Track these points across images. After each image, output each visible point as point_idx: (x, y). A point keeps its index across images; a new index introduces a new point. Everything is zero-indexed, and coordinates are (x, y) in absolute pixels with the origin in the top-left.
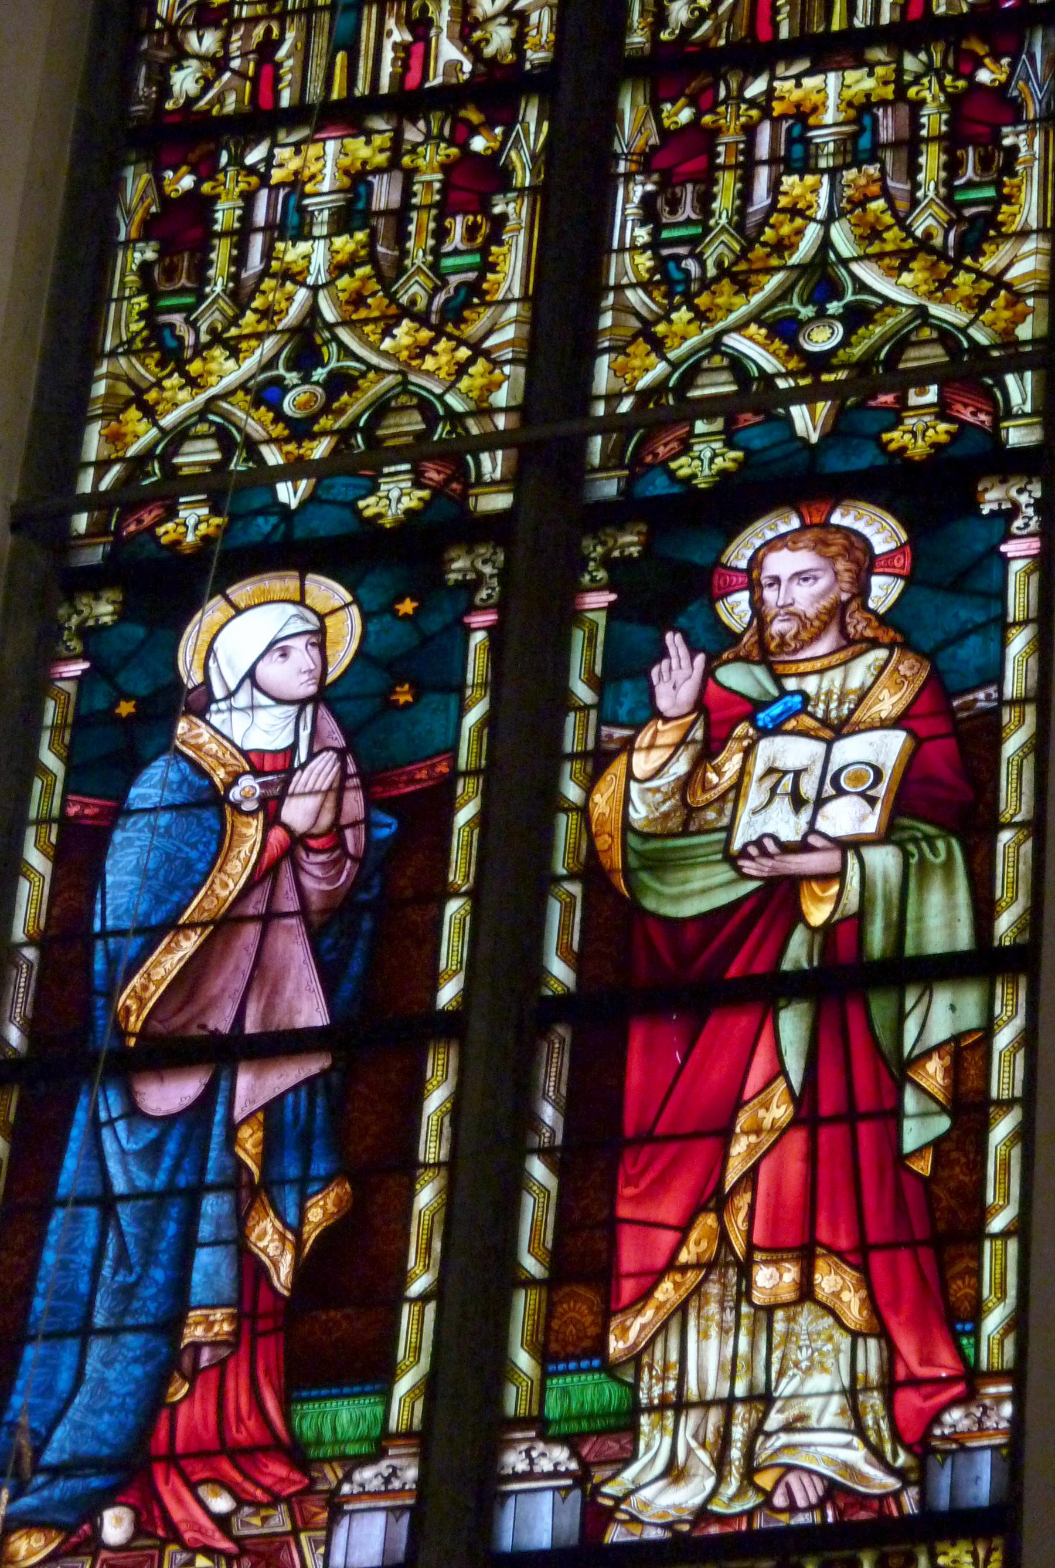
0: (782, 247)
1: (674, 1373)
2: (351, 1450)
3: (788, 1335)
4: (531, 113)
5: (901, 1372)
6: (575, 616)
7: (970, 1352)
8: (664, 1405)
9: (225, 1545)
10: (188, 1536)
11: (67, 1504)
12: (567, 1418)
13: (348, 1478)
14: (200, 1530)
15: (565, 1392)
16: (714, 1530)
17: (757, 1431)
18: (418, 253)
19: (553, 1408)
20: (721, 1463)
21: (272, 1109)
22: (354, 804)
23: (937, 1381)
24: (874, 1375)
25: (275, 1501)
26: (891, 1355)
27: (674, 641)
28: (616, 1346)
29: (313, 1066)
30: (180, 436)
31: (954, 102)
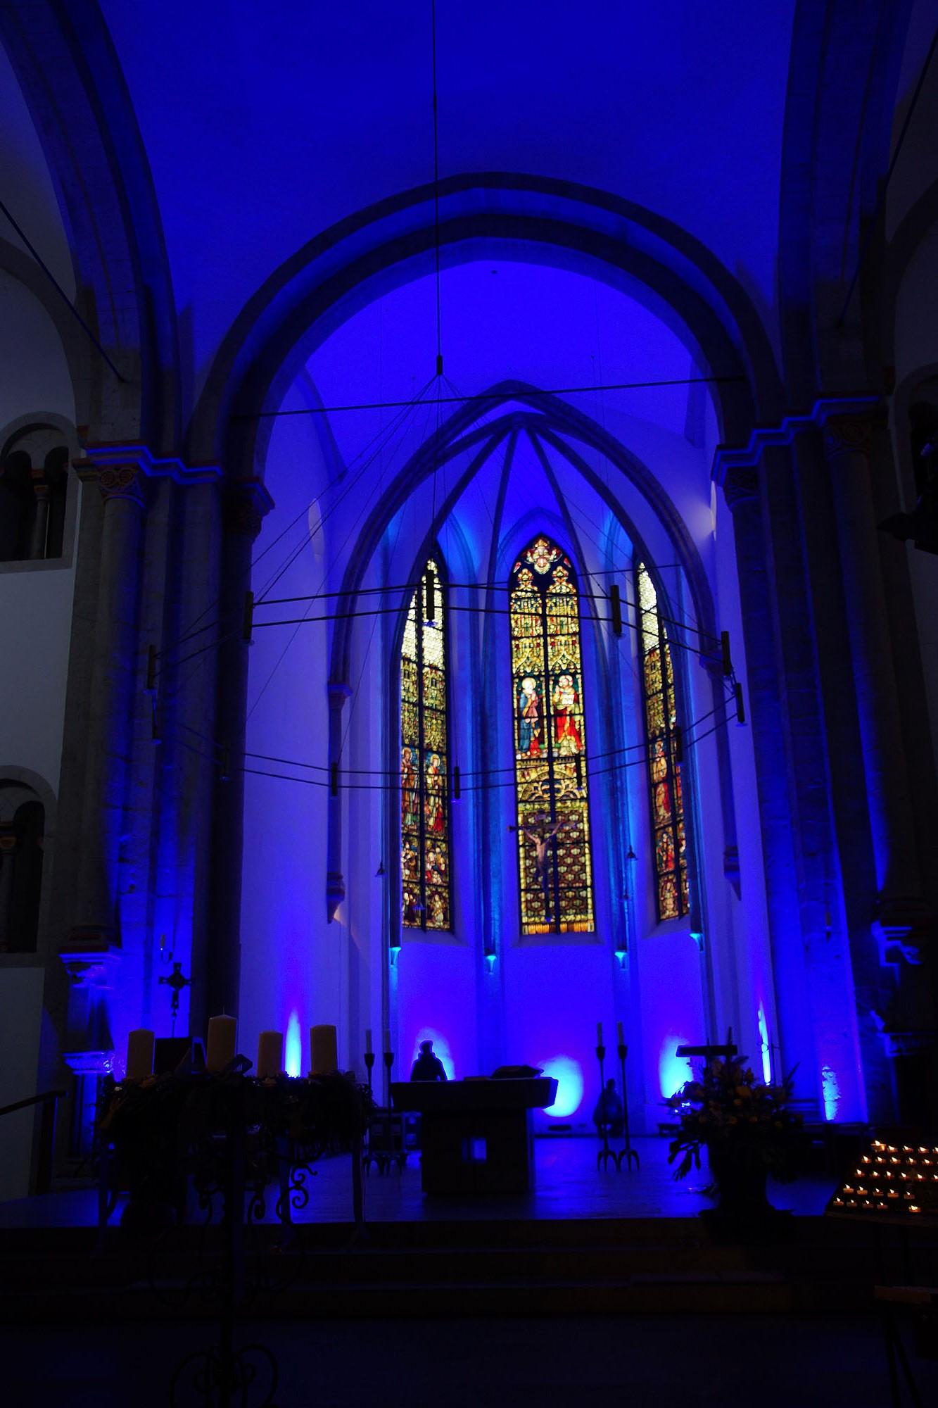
4: (542, 639)
18: (535, 651)
29: (537, 719)
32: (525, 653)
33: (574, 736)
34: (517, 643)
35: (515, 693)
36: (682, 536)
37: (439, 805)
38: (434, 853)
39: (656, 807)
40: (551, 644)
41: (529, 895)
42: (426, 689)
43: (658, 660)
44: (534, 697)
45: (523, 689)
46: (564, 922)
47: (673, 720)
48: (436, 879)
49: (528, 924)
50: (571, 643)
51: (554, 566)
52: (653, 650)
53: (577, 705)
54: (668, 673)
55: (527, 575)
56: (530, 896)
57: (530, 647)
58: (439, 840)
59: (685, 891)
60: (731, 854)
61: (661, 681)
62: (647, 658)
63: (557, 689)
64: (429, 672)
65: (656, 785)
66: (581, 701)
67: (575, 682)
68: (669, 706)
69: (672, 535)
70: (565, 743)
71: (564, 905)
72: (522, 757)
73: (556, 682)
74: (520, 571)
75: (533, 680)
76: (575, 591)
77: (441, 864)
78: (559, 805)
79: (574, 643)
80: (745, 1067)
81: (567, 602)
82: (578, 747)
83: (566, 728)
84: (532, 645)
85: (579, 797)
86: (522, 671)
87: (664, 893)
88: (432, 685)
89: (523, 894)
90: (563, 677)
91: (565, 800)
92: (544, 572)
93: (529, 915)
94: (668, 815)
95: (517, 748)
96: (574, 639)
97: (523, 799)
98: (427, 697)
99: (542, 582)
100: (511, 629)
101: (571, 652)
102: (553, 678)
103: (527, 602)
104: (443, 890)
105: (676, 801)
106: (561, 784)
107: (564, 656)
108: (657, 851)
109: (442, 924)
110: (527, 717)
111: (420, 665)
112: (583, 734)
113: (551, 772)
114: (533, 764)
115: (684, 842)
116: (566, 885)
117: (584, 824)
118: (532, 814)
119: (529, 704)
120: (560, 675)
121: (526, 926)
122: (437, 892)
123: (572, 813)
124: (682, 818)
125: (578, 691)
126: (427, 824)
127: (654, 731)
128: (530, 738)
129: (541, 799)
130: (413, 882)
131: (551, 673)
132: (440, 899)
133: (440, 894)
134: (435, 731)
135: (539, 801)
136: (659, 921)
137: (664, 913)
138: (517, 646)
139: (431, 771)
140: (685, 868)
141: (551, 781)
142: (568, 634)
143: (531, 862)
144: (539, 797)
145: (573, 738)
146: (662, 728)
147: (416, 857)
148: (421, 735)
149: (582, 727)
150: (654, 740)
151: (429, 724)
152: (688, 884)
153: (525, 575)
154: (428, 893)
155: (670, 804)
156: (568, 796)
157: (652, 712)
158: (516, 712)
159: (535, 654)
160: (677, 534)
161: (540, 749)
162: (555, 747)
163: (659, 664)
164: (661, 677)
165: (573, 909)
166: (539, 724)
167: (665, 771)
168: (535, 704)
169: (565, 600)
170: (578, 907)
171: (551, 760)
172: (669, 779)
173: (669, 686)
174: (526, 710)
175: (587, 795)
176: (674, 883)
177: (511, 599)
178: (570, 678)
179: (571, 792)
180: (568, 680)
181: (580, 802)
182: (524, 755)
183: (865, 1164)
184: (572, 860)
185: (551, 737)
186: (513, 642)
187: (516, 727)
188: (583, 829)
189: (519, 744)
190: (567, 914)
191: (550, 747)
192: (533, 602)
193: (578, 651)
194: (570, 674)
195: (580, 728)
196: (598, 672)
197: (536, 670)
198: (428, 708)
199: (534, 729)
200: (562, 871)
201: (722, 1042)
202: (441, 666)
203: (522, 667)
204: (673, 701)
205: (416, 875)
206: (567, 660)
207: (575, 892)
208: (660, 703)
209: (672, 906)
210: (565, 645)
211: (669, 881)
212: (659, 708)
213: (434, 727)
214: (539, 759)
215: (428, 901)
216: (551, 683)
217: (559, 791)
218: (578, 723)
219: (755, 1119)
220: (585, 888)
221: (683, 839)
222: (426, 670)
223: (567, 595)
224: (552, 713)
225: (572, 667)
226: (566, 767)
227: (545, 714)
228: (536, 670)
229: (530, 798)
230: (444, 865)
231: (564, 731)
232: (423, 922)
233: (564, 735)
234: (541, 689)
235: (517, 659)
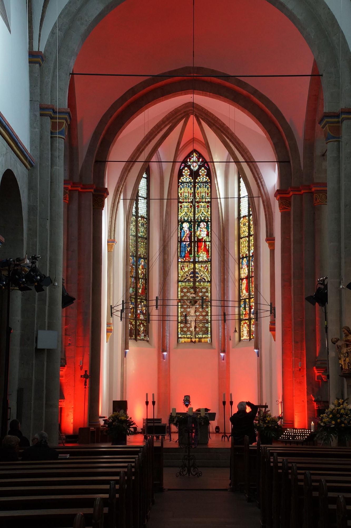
0: (201, 211)
6: (196, 226)
21: (188, 244)
22: (189, 232)
27: (199, 227)
28: (199, 254)
29: (189, 243)
30: (182, 216)
31: (207, 206)
32: (184, 210)
33: (206, 252)
34: (181, 205)
35: (179, 229)
36: (262, 185)
37: (144, 283)
38: (141, 305)
39: (242, 289)
40: (197, 207)
41: (182, 325)
42: (139, 228)
43: (247, 222)
44: (188, 232)
45: (183, 227)
46: (197, 338)
47: (252, 251)
48: (142, 317)
49: (181, 338)
50: (206, 206)
51: (200, 167)
52: (244, 217)
53: (208, 237)
54: (251, 229)
55: (187, 171)
56: (182, 325)
57: (187, 207)
58: (143, 299)
59: (253, 329)
60: (273, 323)
61: (248, 232)
62: (242, 219)
63: (199, 229)
64: (141, 220)
65: (242, 279)
66: (210, 235)
67: (207, 225)
68: (251, 245)
69: (258, 184)
70: (201, 255)
71: (197, 330)
72: (181, 260)
73: (199, 225)
74: (184, 168)
75: (188, 223)
76: (209, 180)
77: (144, 310)
78: (197, 284)
79: (208, 206)
80: (269, 413)
81: (206, 186)
82: (207, 257)
83: (202, 248)
84: (188, 207)
85: (207, 281)
86: (183, 219)
87: (243, 329)
88: (142, 226)
89: (179, 324)
90: (202, 223)
91: (200, 282)
92: (195, 170)
93: (182, 334)
94: (247, 294)
95: (179, 256)
96: (208, 204)
97: (181, 280)
98: (140, 232)
99: (194, 175)
100: (178, 198)
101: (206, 211)
102: (197, 223)
103: (187, 184)
104: (144, 322)
105: (251, 288)
106: (199, 274)
107: (203, 213)
108: (241, 310)
109: (143, 337)
110: (184, 241)
111: (137, 216)
112: (210, 251)
113: (194, 268)
114: (186, 264)
115: (253, 307)
117: (208, 293)
118: (185, 288)
119: (185, 235)
120: (200, 222)
121: (180, 339)
122: (142, 323)
123: (203, 288)
124: (253, 296)
125: (209, 230)
126: (139, 292)
127: (243, 254)
128: (185, 252)
129: (189, 281)
130: (132, 319)
131: (196, 221)
132: (143, 326)
133: (143, 324)
134: (143, 248)
135: (189, 282)
136: (240, 340)
137: (242, 337)
138: (181, 206)
139: (140, 267)
140: (253, 319)
141: (194, 273)
142: (205, 202)
143: (183, 310)
144: (188, 280)
145: (205, 253)
146: (246, 254)
147: (133, 308)
148: (137, 251)
149: (210, 248)
150: (243, 258)
151: (140, 245)
152: (254, 326)
153: (186, 172)
154: (138, 323)
155: (248, 289)
156: (202, 280)
157: (243, 245)
158: (179, 238)
159: (189, 211)
160: (260, 184)
161: (190, 257)
162: (197, 257)
163: (247, 224)
164: (248, 230)
165: (202, 332)
166: (190, 245)
167: (247, 274)
168: (188, 235)
169: (204, 184)
171: (194, 262)
172: (248, 278)
173: (251, 236)
174: (184, 238)
175: (210, 280)
176: (248, 325)
177: (179, 182)
178: (205, 224)
179: (203, 278)
180: (204, 224)
181: (207, 283)
182: (182, 259)
183: (285, 433)
185: (195, 251)
186: (179, 204)
187: (179, 246)
188: (208, 296)
189: (180, 254)
190: (199, 334)
191: (194, 257)
192: (189, 185)
193: (209, 211)
194: (205, 222)
195: (209, 248)
196: (219, 223)
197: (189, 218)
198: (140, 237)
199: (187, 247)
201: (264, 404)
202: (145, 216)
203: (183, 217)
204: (253, 243)
205: (133, 316)
206: (204, 215)
207: (203, 325)
208: (247, 242)
209: (246, 334)
210: (204, 207)
211: (245, 323)
212: (246, 244)
213: (142, 246)
214: (189, 262)
215: (138, 327)
216: (196, 225)
217: (197, 277)
218: (208, 246)
219: (271, 425)
220: (207, 323)
221: (253, 306)
222: (140, 219)
223: (206, 182)
224: (196, 240)
225: (206, 218)
226: (201, 266)
227: (193, 240)
228: (189, 218)
229: (184, 280)
230: (145, 311)
231: (201, 249)
232: (136, 337)
233: (201, 251)
234: (192, 228)
235: (181, 213)
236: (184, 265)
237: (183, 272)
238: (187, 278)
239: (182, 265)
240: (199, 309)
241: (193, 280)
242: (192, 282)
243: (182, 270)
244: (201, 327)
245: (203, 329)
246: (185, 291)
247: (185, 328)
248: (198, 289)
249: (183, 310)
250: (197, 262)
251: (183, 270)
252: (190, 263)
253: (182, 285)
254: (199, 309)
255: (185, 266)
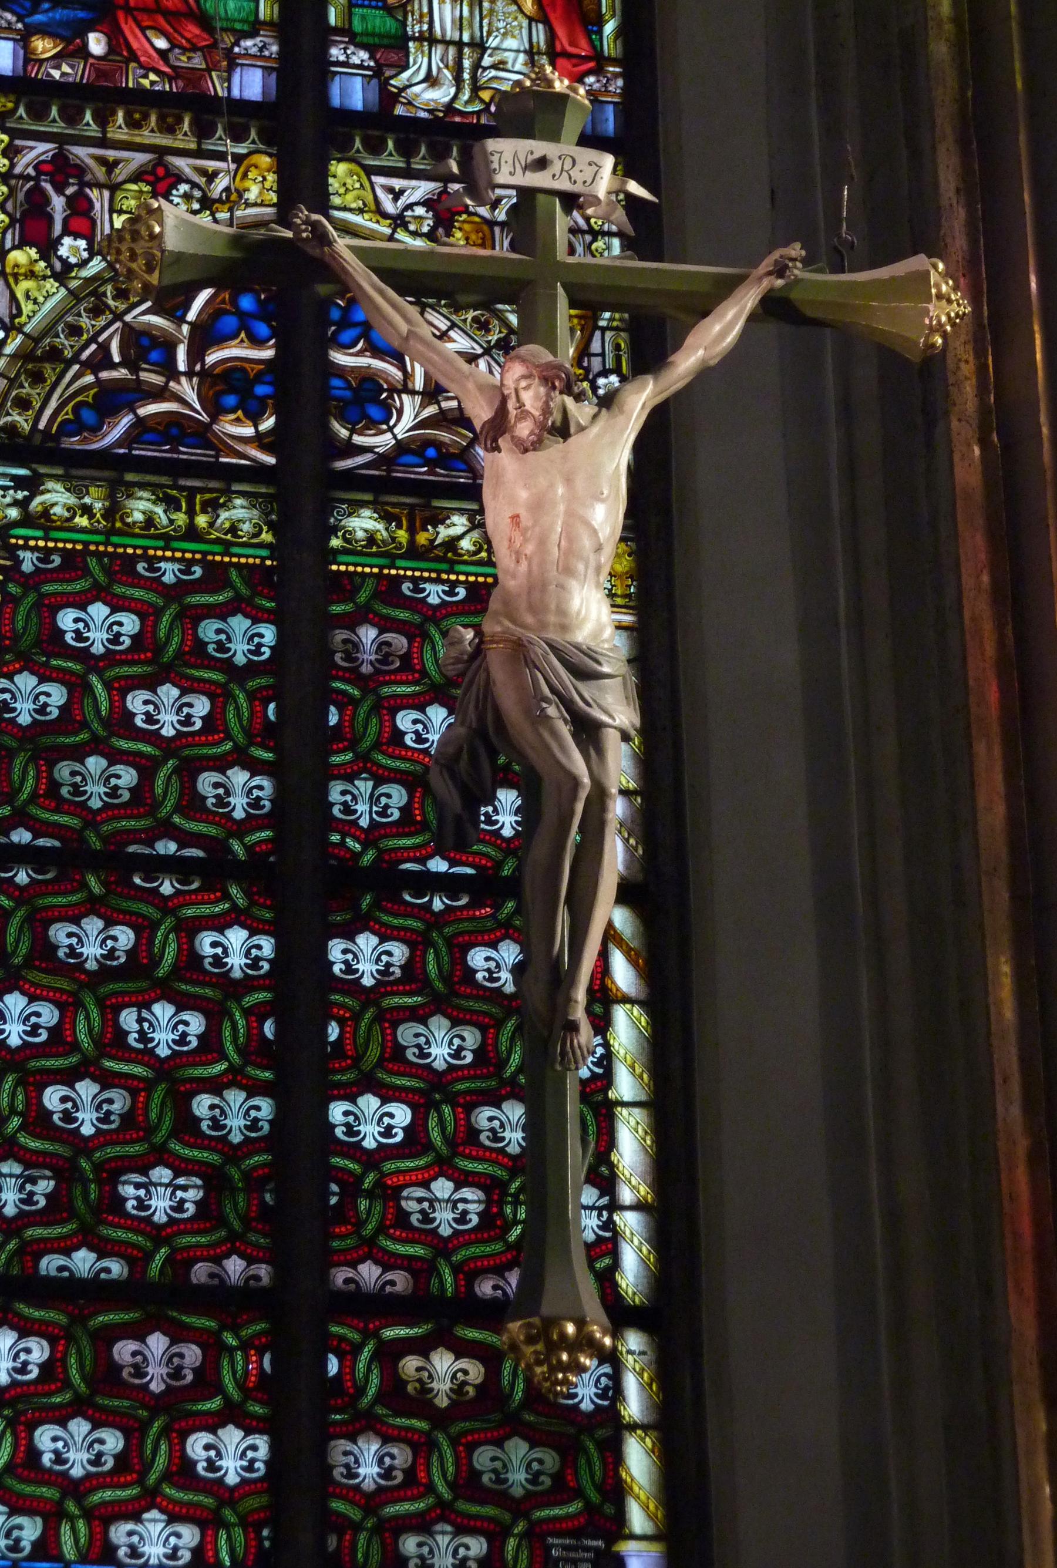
1: (426, 19)
2: (238, 26)
3: (492, 11)
5: (558, 48)
7: (597, 43)
8: (420, 39)
9: (167, 69)
10: (142, 59)
11: (66, 23)
12: (366, 34)
13: (237, 43)
14: (150, 57)
15: (363, 18)
16: (457, 119)
17: (477, 66)
19: (357, 26)
20: (458, 80)
23: (579, 56)
24: (543, 46)
25: (194, 48)
26: (552, 37)
72: (29, 58)
91: (428, 490)
116: (401, 1281)
129: (186, 453)
143: (48, 1015)
165: (463, 1527)
170: (520, 1507)
184: (471, 1037)
200: (370, 1137)
207: (490, 1358)
229: (75, 426)
236: (82, 153)
237: (63, 273)
238: (160, 394)
239: (42, 149)
240: (407, 1034)
241: (259, 440)
242: (256, 473)
243: (48, 248)
244: (443, 1402)
245: (483, 1458)
246: (98, 640)
247: (79, 1427)
248: (385, 625)
249: (48, 1015)
250: (346, 116)
251: (70, 248)
252: (203, 131)
253: (27, 520)
254: (407, 1034)
255: (110, 166)
